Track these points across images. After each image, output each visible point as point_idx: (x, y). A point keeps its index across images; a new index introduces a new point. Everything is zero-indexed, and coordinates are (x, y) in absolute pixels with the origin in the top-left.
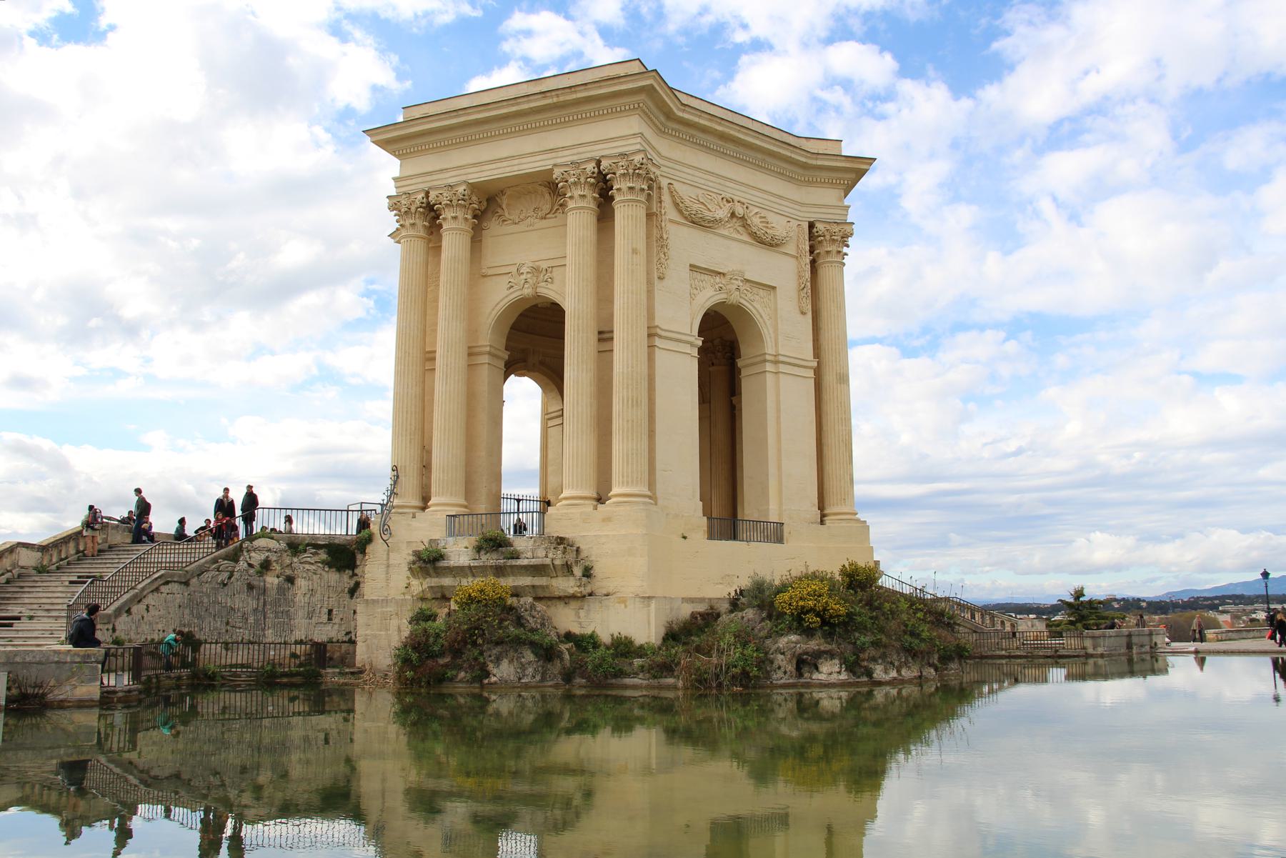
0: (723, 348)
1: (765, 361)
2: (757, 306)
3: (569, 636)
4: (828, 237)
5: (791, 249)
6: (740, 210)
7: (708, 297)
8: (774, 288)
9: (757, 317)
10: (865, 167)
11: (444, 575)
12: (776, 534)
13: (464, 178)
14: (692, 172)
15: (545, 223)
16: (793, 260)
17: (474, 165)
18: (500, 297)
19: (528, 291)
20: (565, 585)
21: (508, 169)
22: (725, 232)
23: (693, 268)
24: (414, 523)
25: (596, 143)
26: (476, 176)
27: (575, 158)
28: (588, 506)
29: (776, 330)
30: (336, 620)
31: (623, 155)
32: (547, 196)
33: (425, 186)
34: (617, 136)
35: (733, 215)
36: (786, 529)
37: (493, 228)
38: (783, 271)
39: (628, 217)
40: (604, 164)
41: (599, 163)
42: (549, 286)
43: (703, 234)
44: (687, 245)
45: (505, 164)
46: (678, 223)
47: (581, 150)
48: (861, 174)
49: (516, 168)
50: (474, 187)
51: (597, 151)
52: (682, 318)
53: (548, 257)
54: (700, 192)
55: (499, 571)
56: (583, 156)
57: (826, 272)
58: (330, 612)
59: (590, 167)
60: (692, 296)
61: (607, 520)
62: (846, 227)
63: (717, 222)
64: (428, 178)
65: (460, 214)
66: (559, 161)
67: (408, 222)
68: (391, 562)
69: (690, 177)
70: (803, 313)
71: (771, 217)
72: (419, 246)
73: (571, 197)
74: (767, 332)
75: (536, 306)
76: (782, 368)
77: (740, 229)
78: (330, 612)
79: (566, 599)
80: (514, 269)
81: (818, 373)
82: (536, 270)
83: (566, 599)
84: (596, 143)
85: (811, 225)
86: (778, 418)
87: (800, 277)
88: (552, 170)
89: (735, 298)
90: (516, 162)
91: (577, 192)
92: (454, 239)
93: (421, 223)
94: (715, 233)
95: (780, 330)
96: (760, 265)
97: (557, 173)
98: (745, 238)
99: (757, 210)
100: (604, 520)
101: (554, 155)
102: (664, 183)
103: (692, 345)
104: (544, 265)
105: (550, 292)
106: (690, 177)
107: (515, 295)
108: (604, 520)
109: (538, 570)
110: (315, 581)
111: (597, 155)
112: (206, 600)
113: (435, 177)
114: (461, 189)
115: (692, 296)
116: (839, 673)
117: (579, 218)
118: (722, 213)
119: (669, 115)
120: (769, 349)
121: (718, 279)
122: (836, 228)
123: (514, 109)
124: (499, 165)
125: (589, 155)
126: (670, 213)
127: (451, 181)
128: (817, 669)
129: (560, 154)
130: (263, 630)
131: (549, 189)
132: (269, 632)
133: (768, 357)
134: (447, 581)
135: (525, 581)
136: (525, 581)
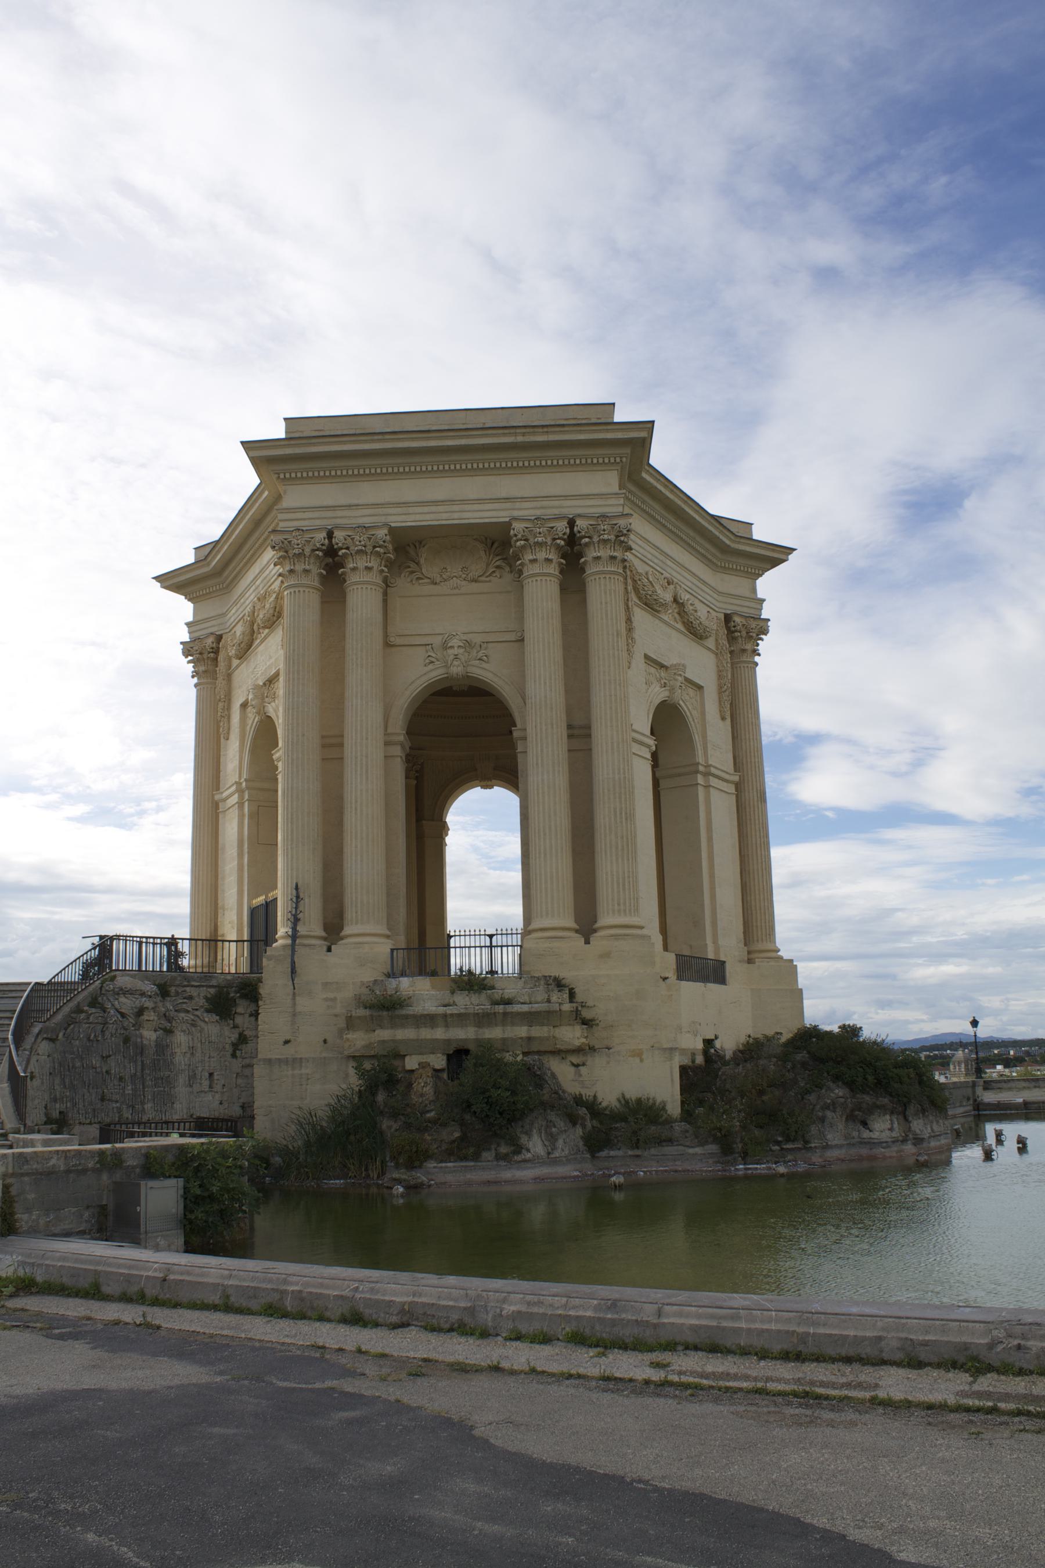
1: (697, 772)
3: (579, 1100)
4: (744, 633)
5: (711, 643)
7: (658, 694)
8: (700, 688)
10: (782, 557)
11: (403, 1026)
13: (383, 519)
14: (651, 544)
15: (475, 587)
16: (713, 656)
17: (399, 504)
18: (417, 674)
19: (457, 670)
20: (572, 1035)
21: (445, 516)
22: (666, 618)
23: (646, 657)
24: (331, 958)
25: (566, 497)
26: (399, 520)
27: (538, 512)
29: (704, 736)
30: (218, 1087)
31: (604, 517)
32: (482, 553)
33: (329, 524)
36: (728, 966)
37: (402, 584)
39: (604, 593)
40: (580, 523)
41: (572, 523)
42: (484, 665)
45: (441, 508)
47: (545, 503)
48: (775, 562)
49: (456, 516)
50: (392, 531)
51: (570, 508)
54: (648, 568)
55: (483, 1019)
56: (549, 511)
58: (211, 1075)
59: (562, 526)
61: (606, 955)
62: (762, 624)
63: (664, 605)
64: (329, 514)
65: (374, 563)
66: (516, 513)
67: (299, 567)
68: (299, 1009)
70: (723, 719)
71: (699, 606)
72: (313, 598)
73: (534, 561)
74: (697, 738)
75: (451, 687)
76: (714, 782)
77: (676, 615)
78: (211, 1075)
79: (560, 1053)
80: (437, 641)
82: (468, 645)
83: (560, 1053)
84: (566, 497)
85: (728, 618)
86: (710, 839)
87: (720, 677)
88: (508, 525)
90: (455, 508)
91: (541, 555)
92: (363, 597)
93: (316, 570)
94: (660, 619)
97: (518, 527)
98: (680, 626)
100: (601, 956)
101: (508, 505)
103: (649, 746)
104: (477, 639)
105: (492, 672)
107: (436, 673)
108: (601, 956)
109: (531, 1018)
111: (571, 512)
112: (78, 1064)
113: (339, 513)
114: (382, 533)
116: (891, 1129)
117: (542, 590)
118: (668, 597)
122: (753, 624)
123: (463, 442)
124: (434, 509)
125: (556, 511)
127: (366, 521)
128: (865, 1124)
129: (518, 505)
130: (143, 1103)
131: (498, 545)
132: (148, 1106)
133: (701, 768)
134: (404, 1034)
135: (522, 1031)
136: (522, 1031)
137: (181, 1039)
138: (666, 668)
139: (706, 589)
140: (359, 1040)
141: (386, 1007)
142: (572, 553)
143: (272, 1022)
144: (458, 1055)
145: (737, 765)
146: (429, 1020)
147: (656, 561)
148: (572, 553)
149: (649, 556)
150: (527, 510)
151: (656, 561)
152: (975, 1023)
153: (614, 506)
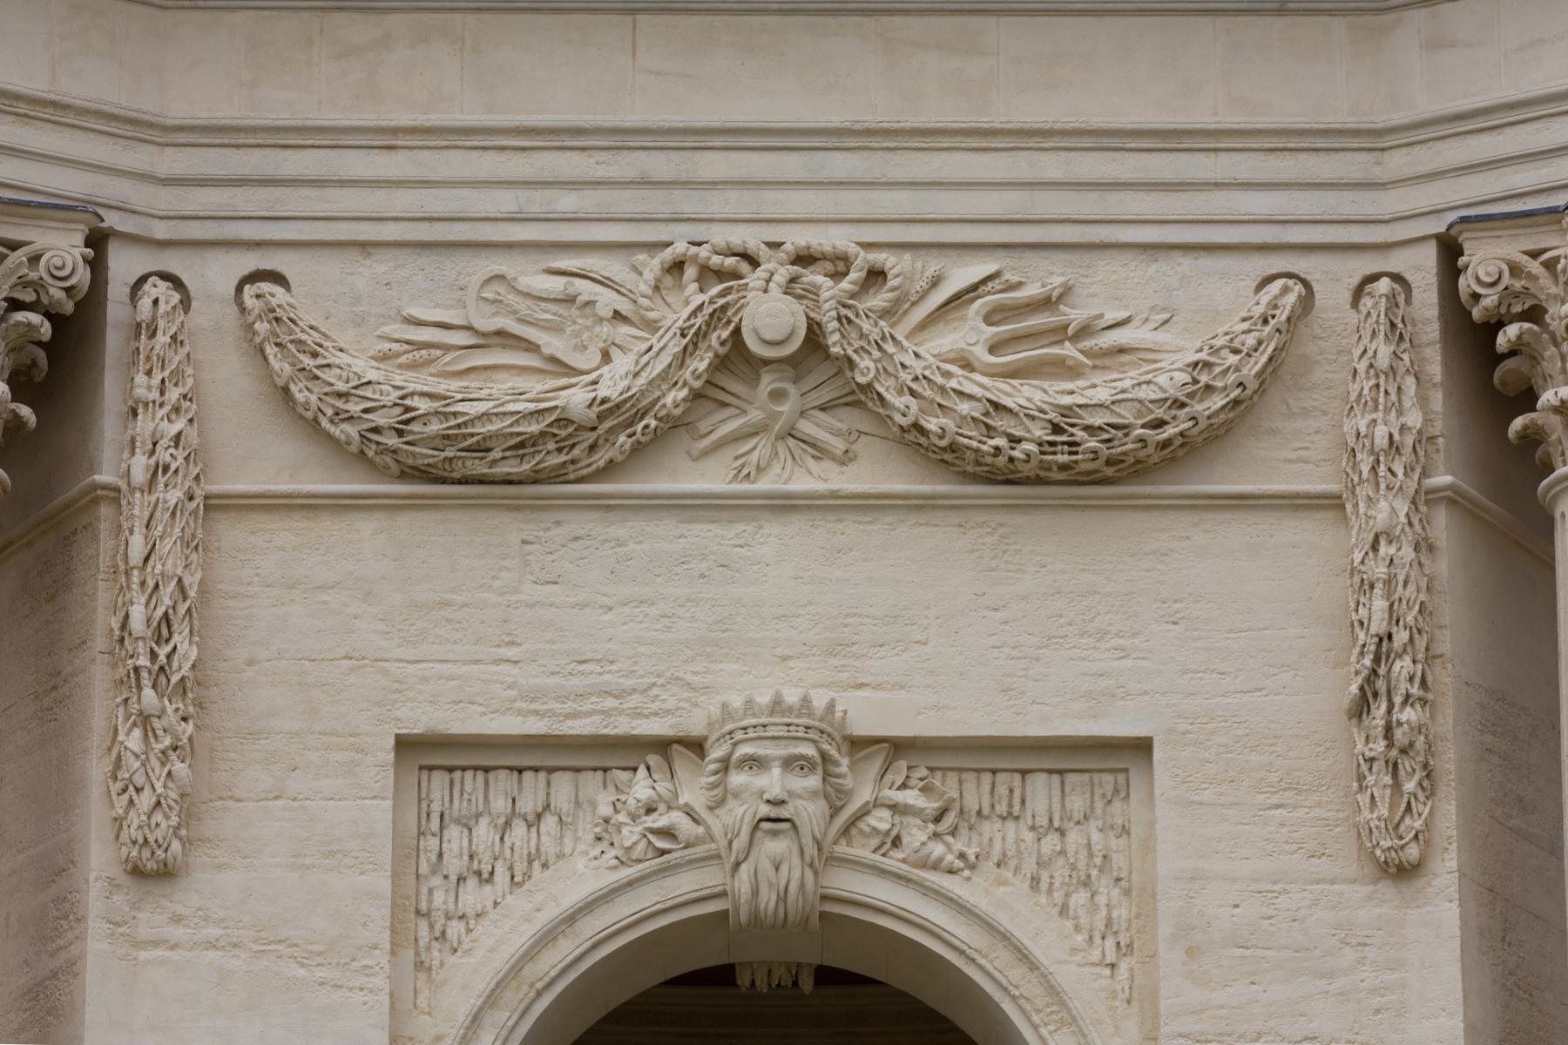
6: (770, 315)
9: (992, 973)
22: (712, 478)
23: (419, 752)
35: (737, 358)
43: (511, 530)
46: (310, 505)
60: (417, 931)
69: (405, 201)
89: (770, 878)
96: (960, 628)
99: (963, 274)
102: (213, 276)
106: (405, 201)
115: (417, 931)
121: (641, 788)
138: (697, 746)
147: (568, 202)
149: (505, 201)
151: (568, 202)
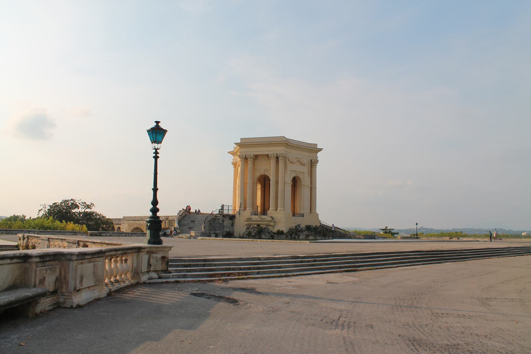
0: (295, 181)
2: (301, 176)
7: (293, 175)
12: (303, 215)
14: (293, 154)
18: (258, 174)
19: (263, 174)
20: (272, 224)
28: (274, 212)
34: (280, 150)
38: (305, 169)
44: (290, 167)
50: (254, 155)
51: (277, 152)
52: (289, 180)
53: (268, 168)
57: (313, 169)
74: (303, 181)
81: (311, 187)
89: (298, 175)
95: (305, 180)
110: (227, 222)
118: (296, 161)
119: (288, 145)
120: (303, 184)
126: (288, 161)
137: (225, 222)
139: (306, 157)
140: (246, 223)
141: (249, 219)
142: (277, 158)
143: (237, 220)
144: (258, 225)
145: (311, 184)
146: (254, 221)
148: (277, 158)
150: (272, 153)
152: (417, 224)
153: (283, 152)
